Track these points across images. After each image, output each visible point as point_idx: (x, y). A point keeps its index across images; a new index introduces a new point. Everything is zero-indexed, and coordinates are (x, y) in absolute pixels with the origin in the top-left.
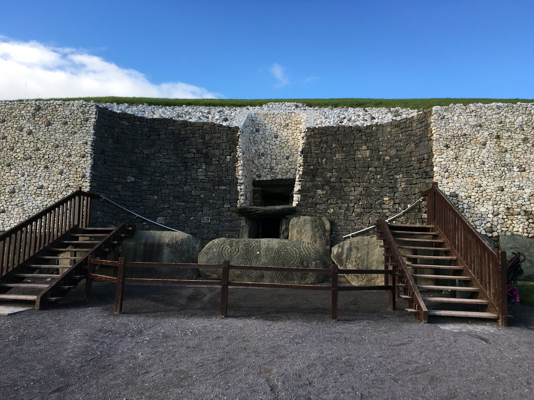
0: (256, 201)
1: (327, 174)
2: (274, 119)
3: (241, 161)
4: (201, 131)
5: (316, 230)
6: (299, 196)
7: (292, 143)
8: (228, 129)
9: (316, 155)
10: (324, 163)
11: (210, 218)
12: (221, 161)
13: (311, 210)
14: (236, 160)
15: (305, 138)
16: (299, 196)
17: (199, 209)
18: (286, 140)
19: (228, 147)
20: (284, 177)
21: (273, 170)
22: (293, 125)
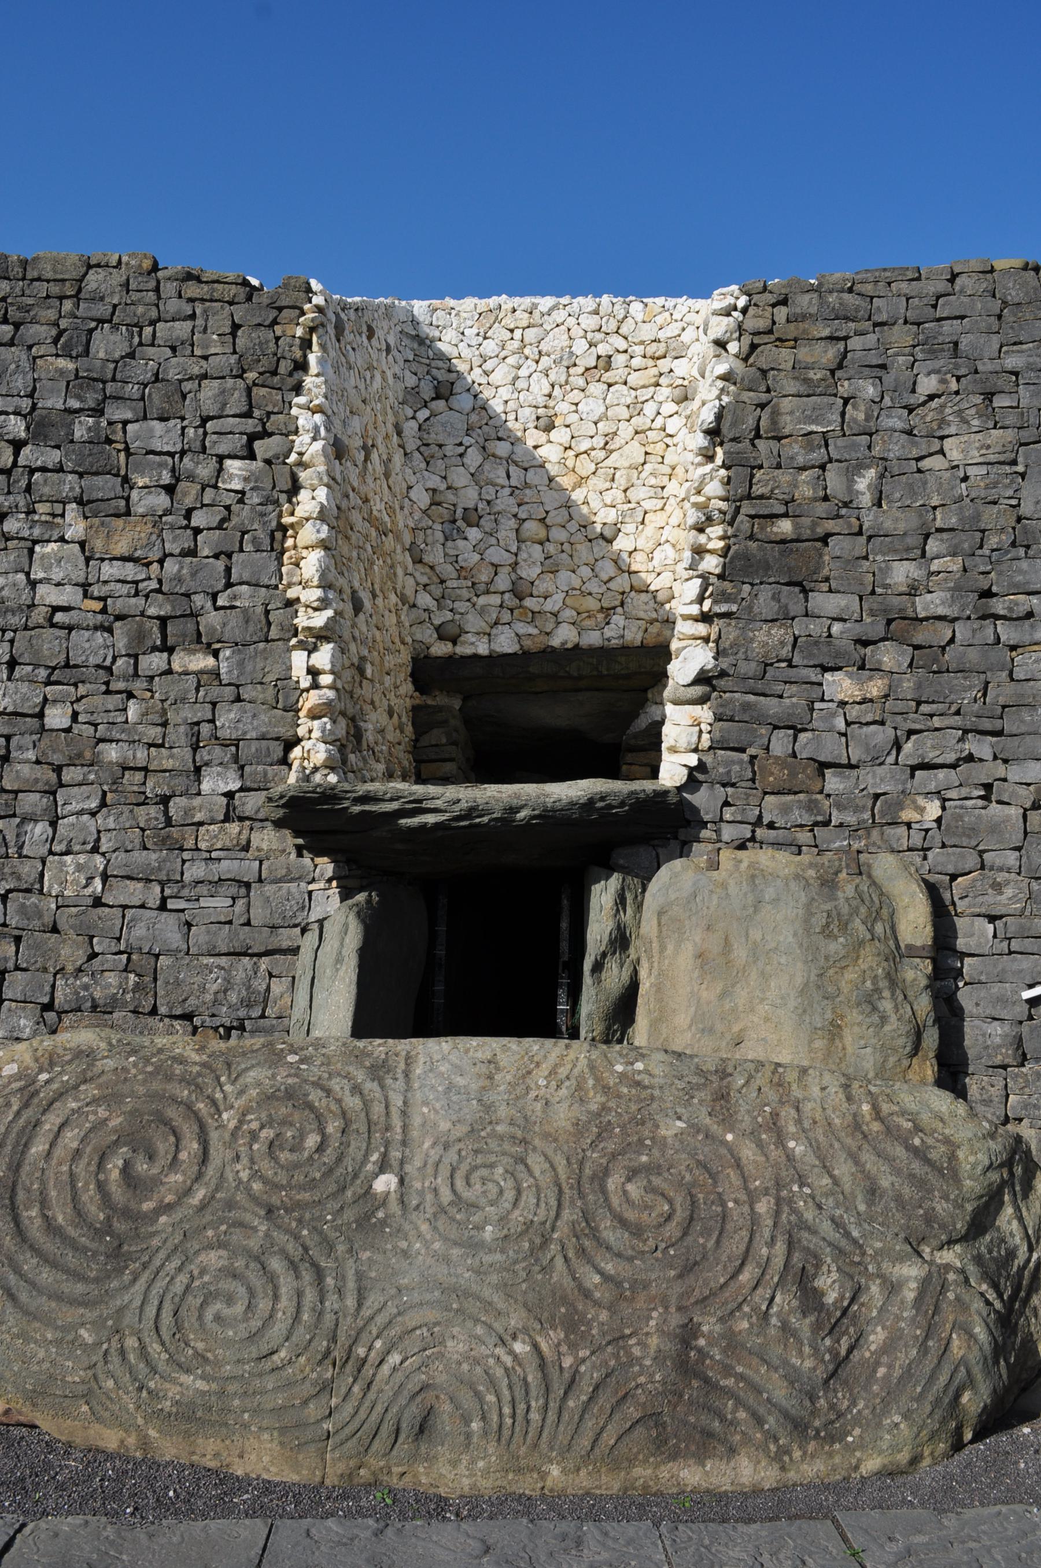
0: (426, 770)
1: (886, 571)
2: (531, 335)
3: (322, 493)
4: (68, 305)
5: (836, 947)
6: (705, 713)
7: (634, 452)
8: (242, 292)
9: (810, 448)
10: (866, 500)
11: (99, 861)
12: (188, 493)
13: (785, 810)
14: (285, 484)
15: (733, 347)
16: (705, 713)
17: (30, 802)
18: (599, 442)
19: (237, 403)
20: (592, 639)
21: (528, 602)
22: (637, 362)
